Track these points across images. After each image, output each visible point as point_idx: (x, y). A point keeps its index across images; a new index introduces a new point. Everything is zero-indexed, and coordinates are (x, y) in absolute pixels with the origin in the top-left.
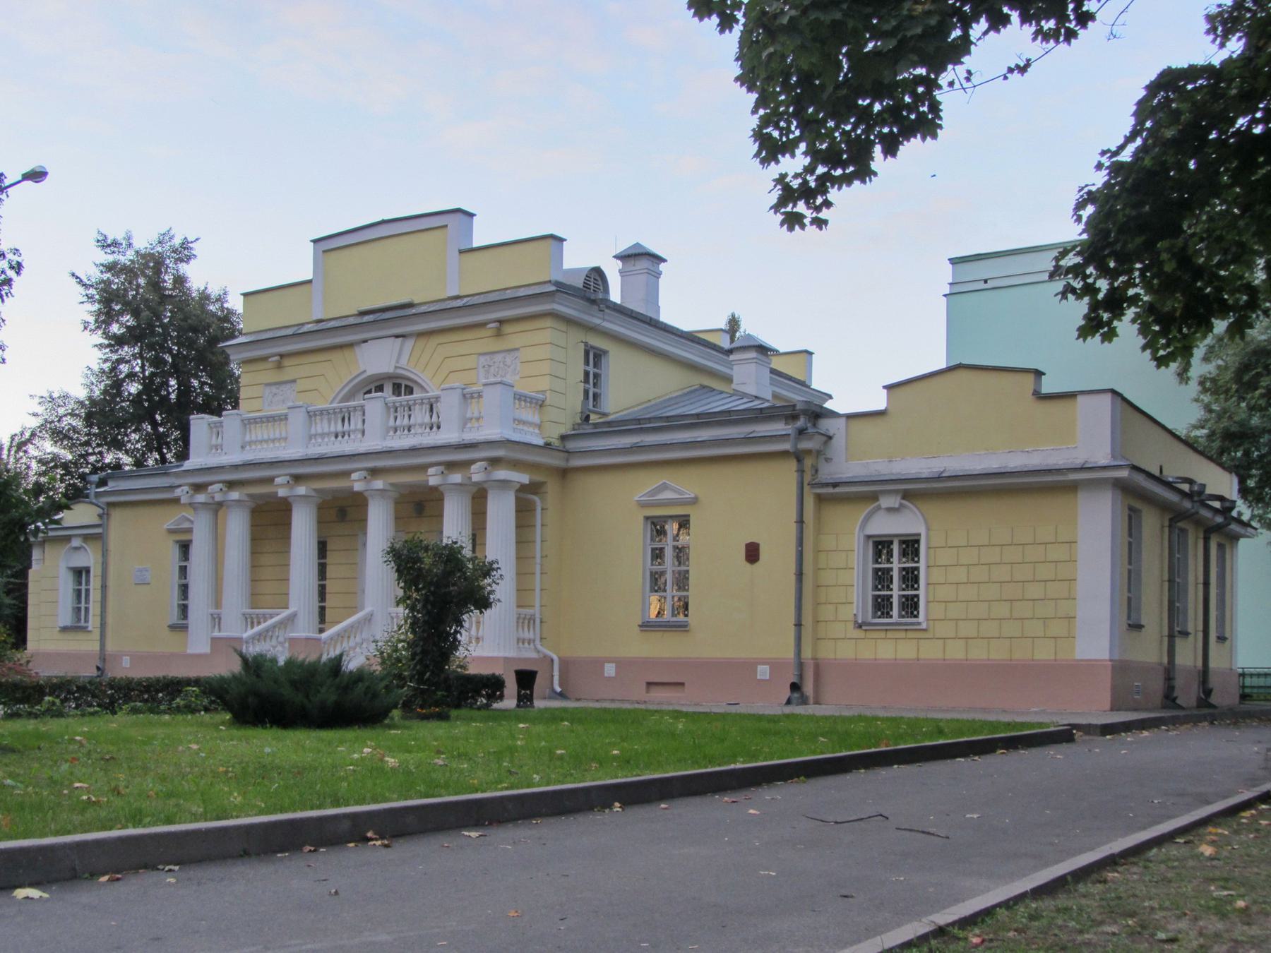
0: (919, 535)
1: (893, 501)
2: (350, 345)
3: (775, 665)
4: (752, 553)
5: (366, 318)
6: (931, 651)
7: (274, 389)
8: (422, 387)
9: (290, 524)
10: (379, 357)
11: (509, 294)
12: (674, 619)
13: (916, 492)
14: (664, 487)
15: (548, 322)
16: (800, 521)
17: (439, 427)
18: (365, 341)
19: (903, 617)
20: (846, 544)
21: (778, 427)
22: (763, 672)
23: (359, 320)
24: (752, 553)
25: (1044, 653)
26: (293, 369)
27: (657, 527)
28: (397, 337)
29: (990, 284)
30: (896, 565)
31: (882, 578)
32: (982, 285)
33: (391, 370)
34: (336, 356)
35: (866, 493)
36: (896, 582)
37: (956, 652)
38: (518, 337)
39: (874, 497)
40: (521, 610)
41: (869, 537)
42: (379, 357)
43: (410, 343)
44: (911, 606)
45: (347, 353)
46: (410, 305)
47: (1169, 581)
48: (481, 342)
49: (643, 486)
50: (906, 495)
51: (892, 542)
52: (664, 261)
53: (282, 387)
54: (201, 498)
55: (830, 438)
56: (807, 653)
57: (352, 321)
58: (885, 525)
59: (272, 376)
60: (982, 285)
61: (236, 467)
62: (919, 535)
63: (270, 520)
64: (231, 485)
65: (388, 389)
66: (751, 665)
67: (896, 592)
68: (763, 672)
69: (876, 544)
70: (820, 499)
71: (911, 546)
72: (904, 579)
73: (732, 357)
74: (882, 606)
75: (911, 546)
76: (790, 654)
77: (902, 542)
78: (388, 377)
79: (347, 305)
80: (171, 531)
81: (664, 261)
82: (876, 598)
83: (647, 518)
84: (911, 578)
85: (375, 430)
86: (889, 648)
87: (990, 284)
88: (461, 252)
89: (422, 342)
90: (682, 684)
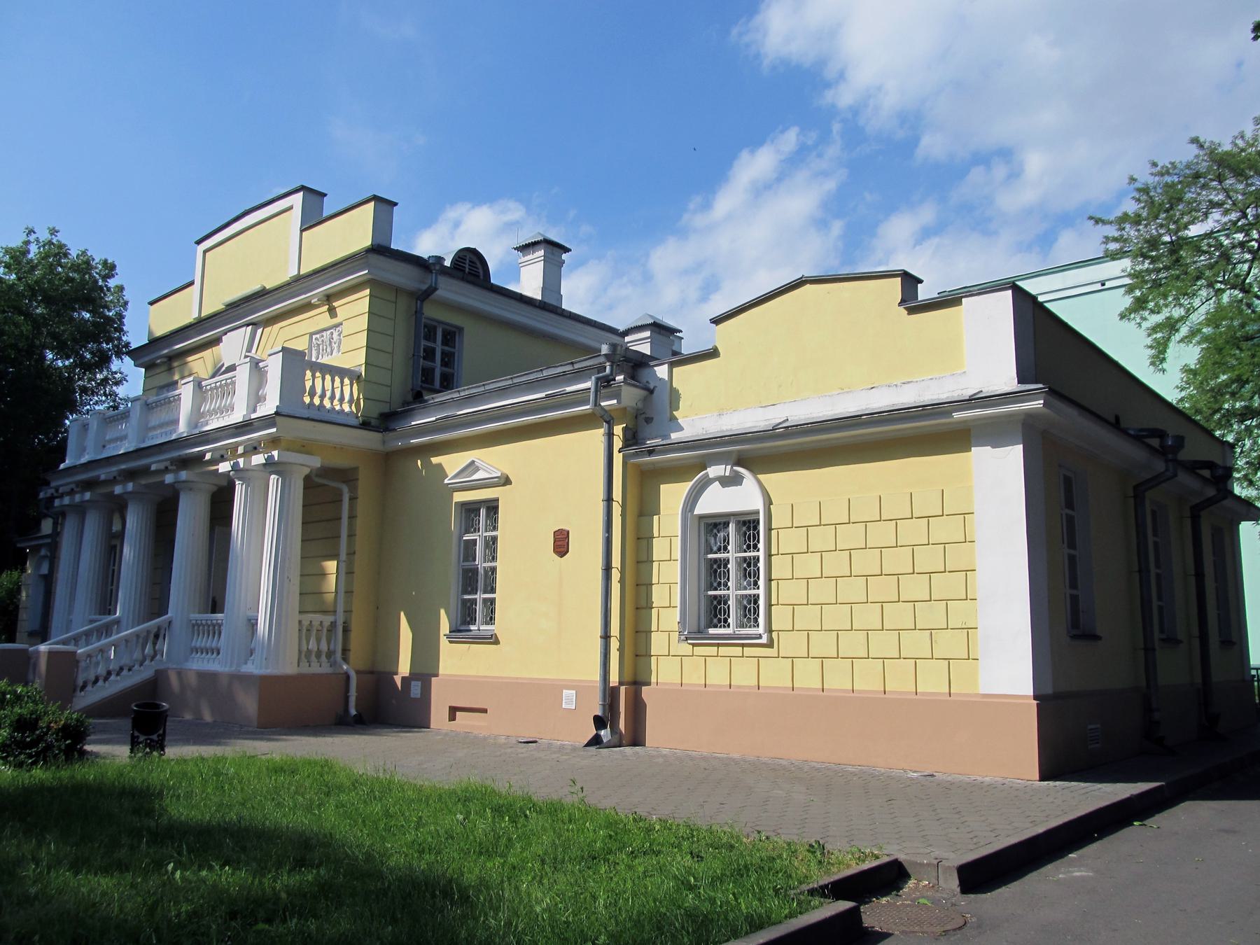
0: (757, 512)
4: (561, 544)
6: (775, 674)
19: (742, 626)
22: (569, 695)
24: (561, 544)
25: (932, 682)
30: (733, 555)
31: (715, 572)
37: (808, 677)
44: (749, 609)
47: (1140, 571)
50: (741, 461)
51: (726, 525)
52: (567, 250)
55: (651, 392)
58: (716, 501)
62: (757, 512)
67: (733, 592)
68: (569, 695)
69: (708, 525)
73: (627, 339)
74: (715, 612)
75: (748, 524)
76: (597, 676)
77: (738, 523)
81: (567, 250)
84: (749, 569)
90: (485, 711)
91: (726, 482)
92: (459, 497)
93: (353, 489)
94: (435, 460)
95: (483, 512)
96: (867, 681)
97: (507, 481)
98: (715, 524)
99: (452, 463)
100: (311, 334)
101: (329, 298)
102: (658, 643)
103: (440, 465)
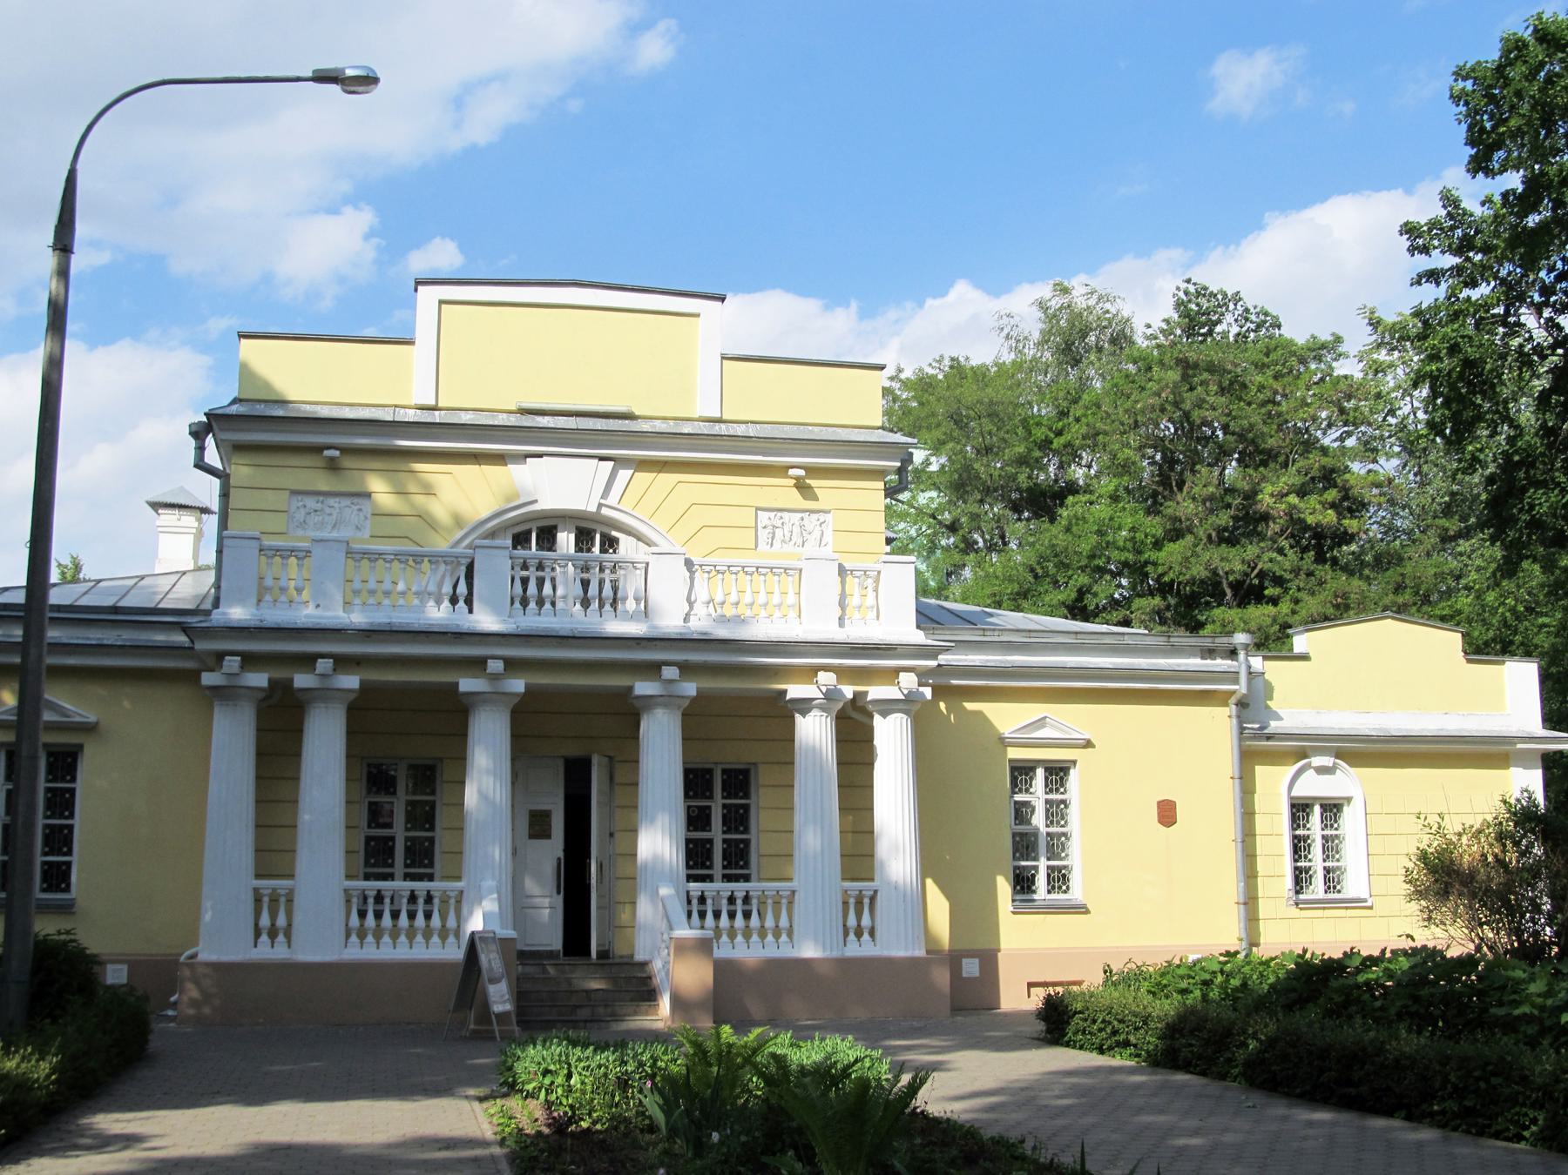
1: (1327, 761)
4: (1167, 812)
7: (311, 503)
8: (639, 537)
9: (301, 731)
12: (1053, 896)
18: (540, 456)
23: (513, 420)
24: (1167, 812)
40: (847, 884)
53: (332, 501)
57: (502, 420)
59: (323, 482)
61: (368, 634)
65: (566, 540)
89: (644, 478)
91: (1322, 770)
92: (1014, 753)
94: (970, 706)
95: (1040, 772)
97: (1088, 744)
99: (1007, 717)
100: (758, 509)
101: (813, 471)
102: (1264, 908)
103: (980, 713)
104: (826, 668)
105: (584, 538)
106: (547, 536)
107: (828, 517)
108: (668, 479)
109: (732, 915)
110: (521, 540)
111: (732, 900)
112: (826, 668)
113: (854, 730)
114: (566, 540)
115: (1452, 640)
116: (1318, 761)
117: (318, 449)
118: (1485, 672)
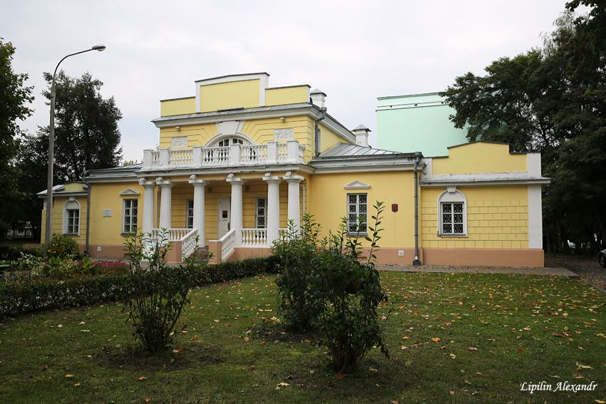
1: (453, 190)
2: (214, 123)
3: (406, 251)
5: (222, 113)
6: (469, 245)
7: (176, 139)
10: (228, 128)
11: (289, 107)
13: (461, 186)
14: (356, 182)
15: (306, 118)
16: (416, 197)
17: (255, 158)
19: (457, 232)
20: (433, 203)
21: (405, 161)
22: (401, 253)
26: (185, 132)
27: (352, 198)
28: (236, 121)
29: (393, 108)
32: (390, 108)
33: (234, 134)
34: (207, 127)
35: (442, 187)
36: (453, 219)
37: (480, 246)
38: (291, 123)
39: (445, 188)
41: (441, 203)
42: (228, 128)
43: (242, 124)
44: (459, 228)
45: (212, 126)
46: (242, 109)
48: (277, 124)
49: (347, 181)
50: (458, 188)
54: (149, 183)
56: (419, 246)
58: (448, 198)
60: (390, 108)
63: (182, 193)
64: (164, 178)
66: (397, 250)
70: (422, 188)
71: (459, 206)
72: (455, 219)
74: (447, 228)
75: (459, 206)
78: (231, 136)
79: (213, 107)
80: (122, 195)
82: (444, 225)
83: (348, 194)
85: (236, 157)
86: (452, 244)
87: (393, 108)
88: (266, 89)
89: (248, 123)
93: (306, 187)
96: (497, 246)
98: (446, 207)
104: (268, 172)
105: (235, 141)
106: (227, 141)
107: (291, 130)
108: (253, 123)
109: (260, 237)
110: (221, 144)
111: (260, 233)
112: (268, 172)
113: (283, 188)
114: (231, 142)
115: (506, 147)
116: (450, 190)
117: (174, 127)
118: (518, 159)
